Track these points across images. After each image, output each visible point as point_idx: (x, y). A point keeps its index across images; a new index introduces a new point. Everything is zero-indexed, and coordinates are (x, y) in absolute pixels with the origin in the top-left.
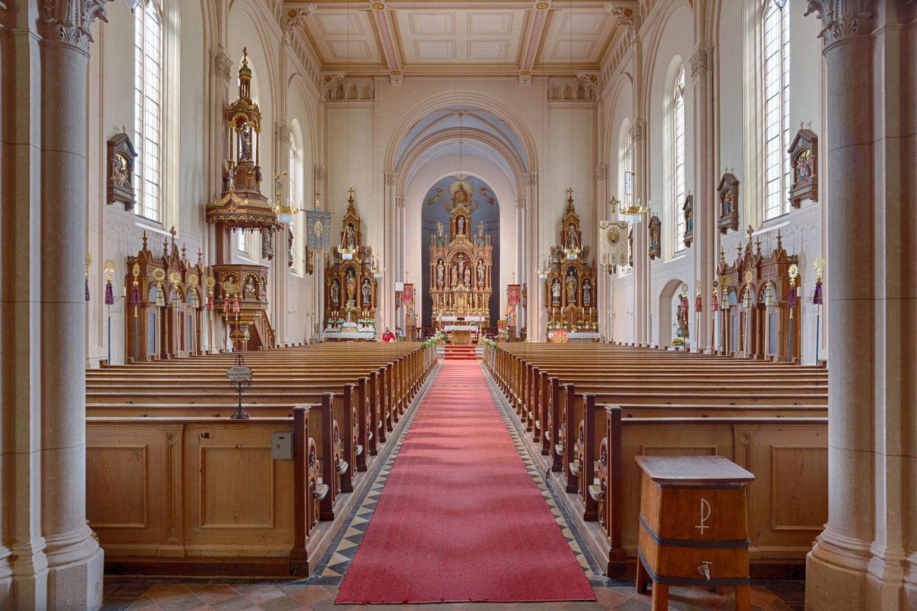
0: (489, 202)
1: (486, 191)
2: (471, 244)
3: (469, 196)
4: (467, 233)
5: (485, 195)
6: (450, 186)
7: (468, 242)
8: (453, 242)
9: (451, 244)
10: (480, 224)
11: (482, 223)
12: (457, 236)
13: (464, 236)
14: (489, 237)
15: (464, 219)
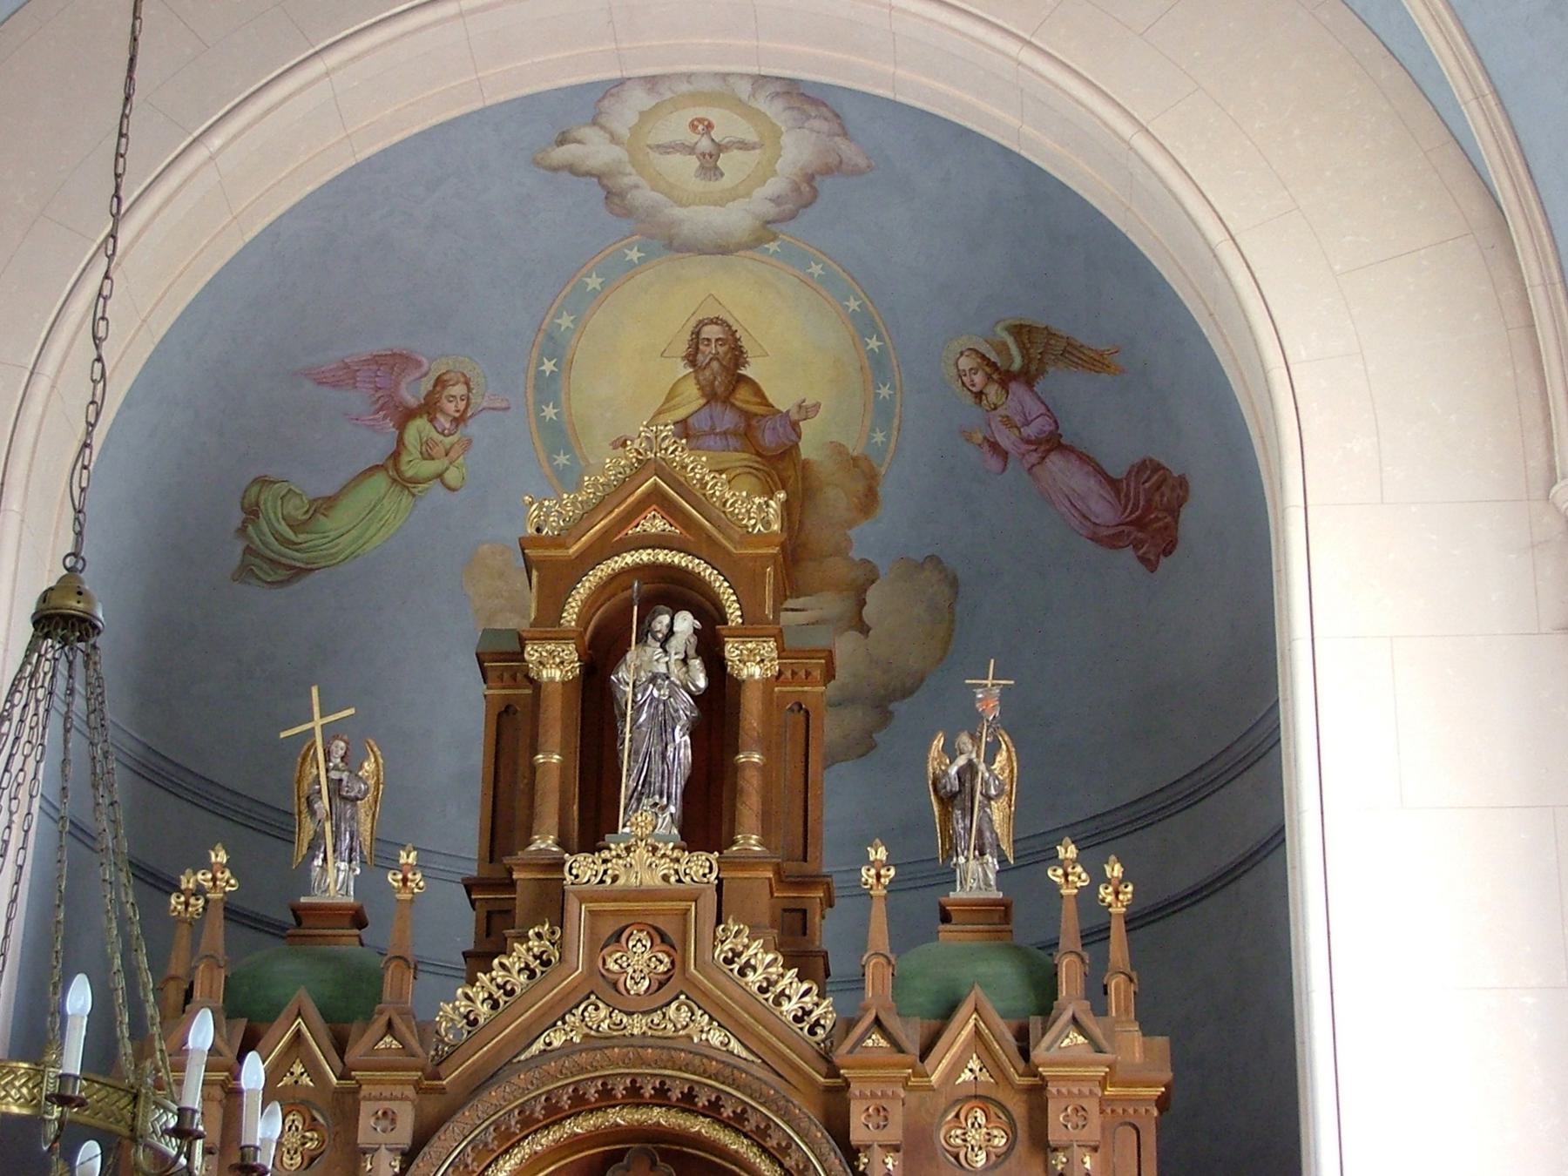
0: (1112, 541)
1: (1061, 383)
2: (796, 993)
3: (836, 498)
4: (750, 842)
5: (1052, 443)
6: (555, 346)
7: (762, 959)
8: (511, 967)
9: (474, 999)
10: (972, 722)
11: (988, 694)
12: (583, 868)
13: (699, 866)
14: (1117, 899)
15: (709, 647)
